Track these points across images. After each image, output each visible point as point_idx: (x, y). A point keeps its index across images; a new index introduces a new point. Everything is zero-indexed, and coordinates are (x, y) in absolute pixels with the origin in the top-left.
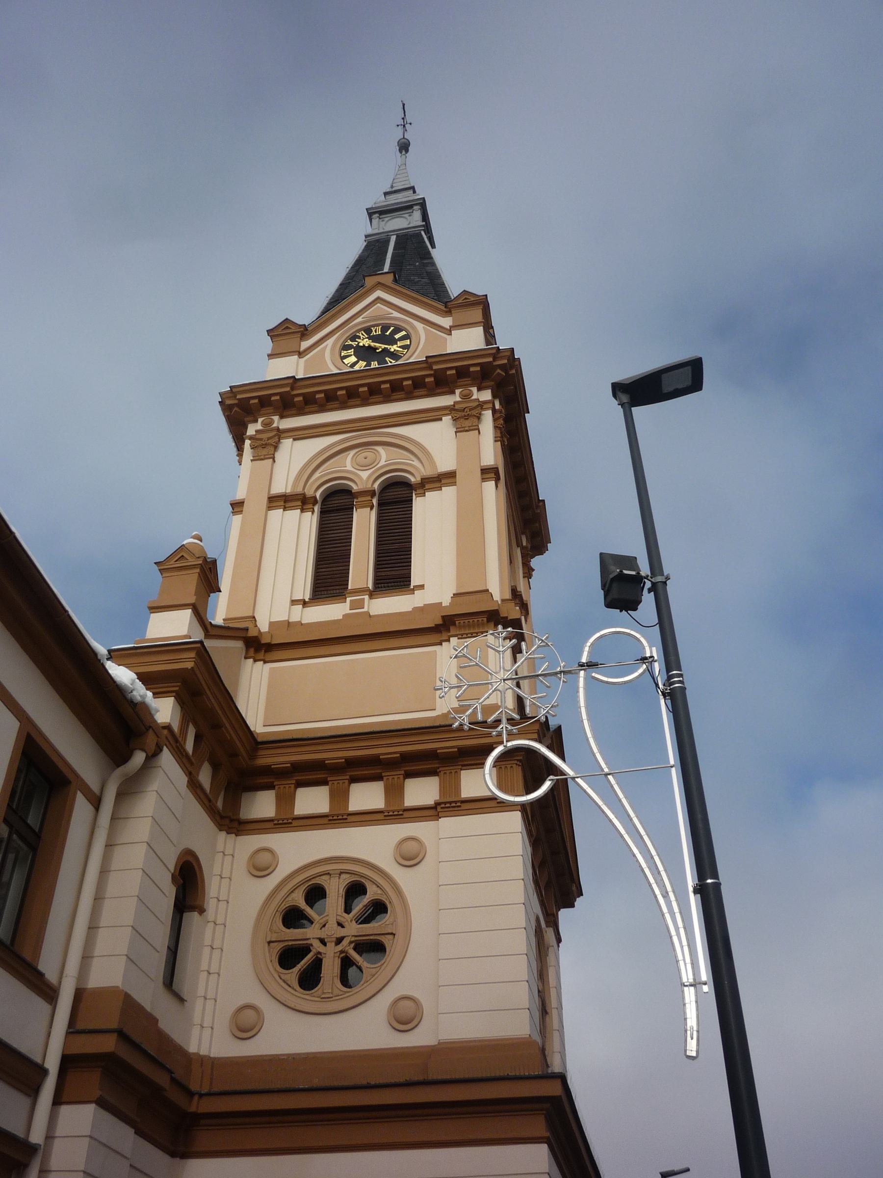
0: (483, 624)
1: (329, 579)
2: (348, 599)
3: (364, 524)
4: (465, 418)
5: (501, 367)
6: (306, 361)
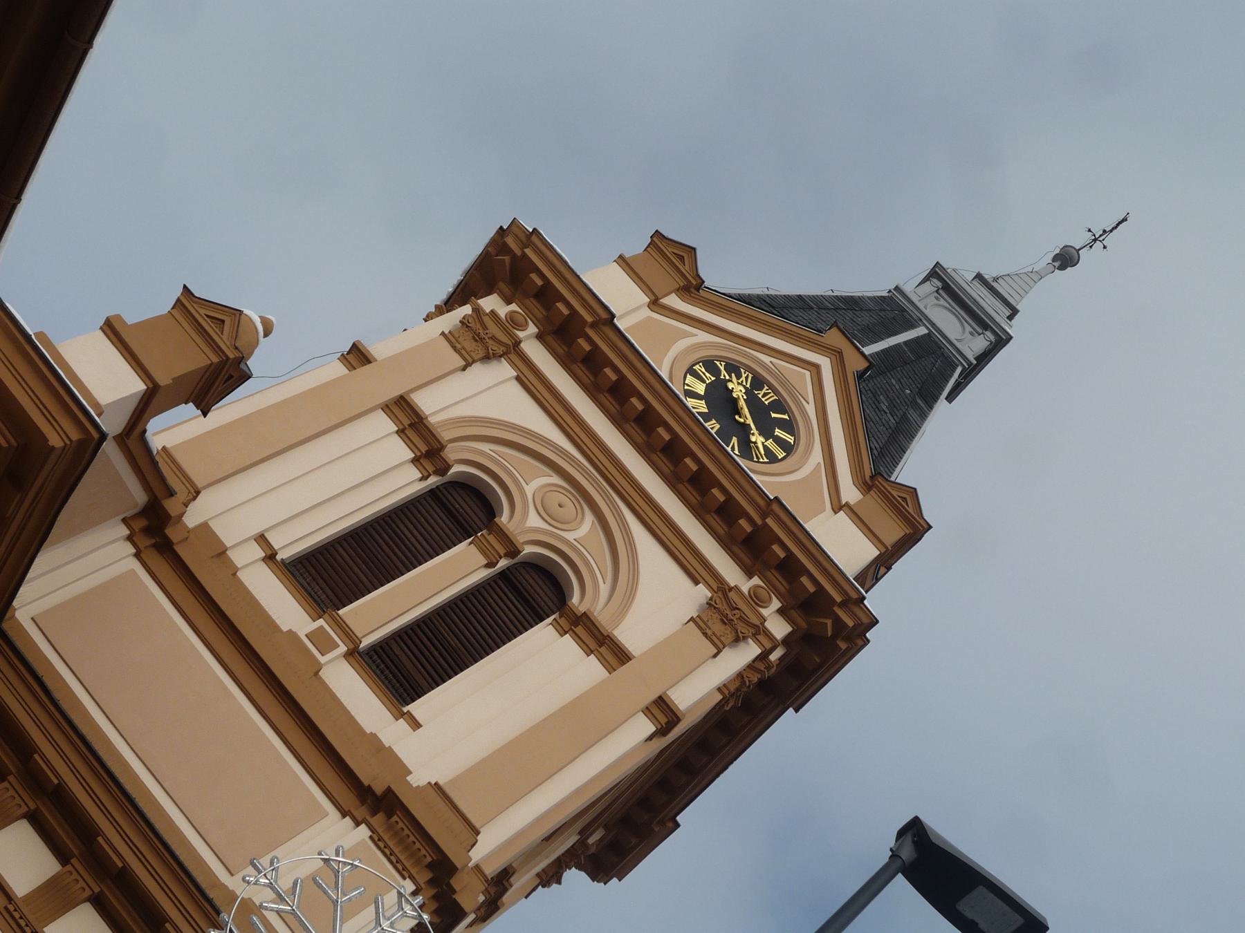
0: (418, 862)
2: (321, 622)
3: (457, 570)
4: (723, 619)
5: (838, 622)
6: (649, 318)
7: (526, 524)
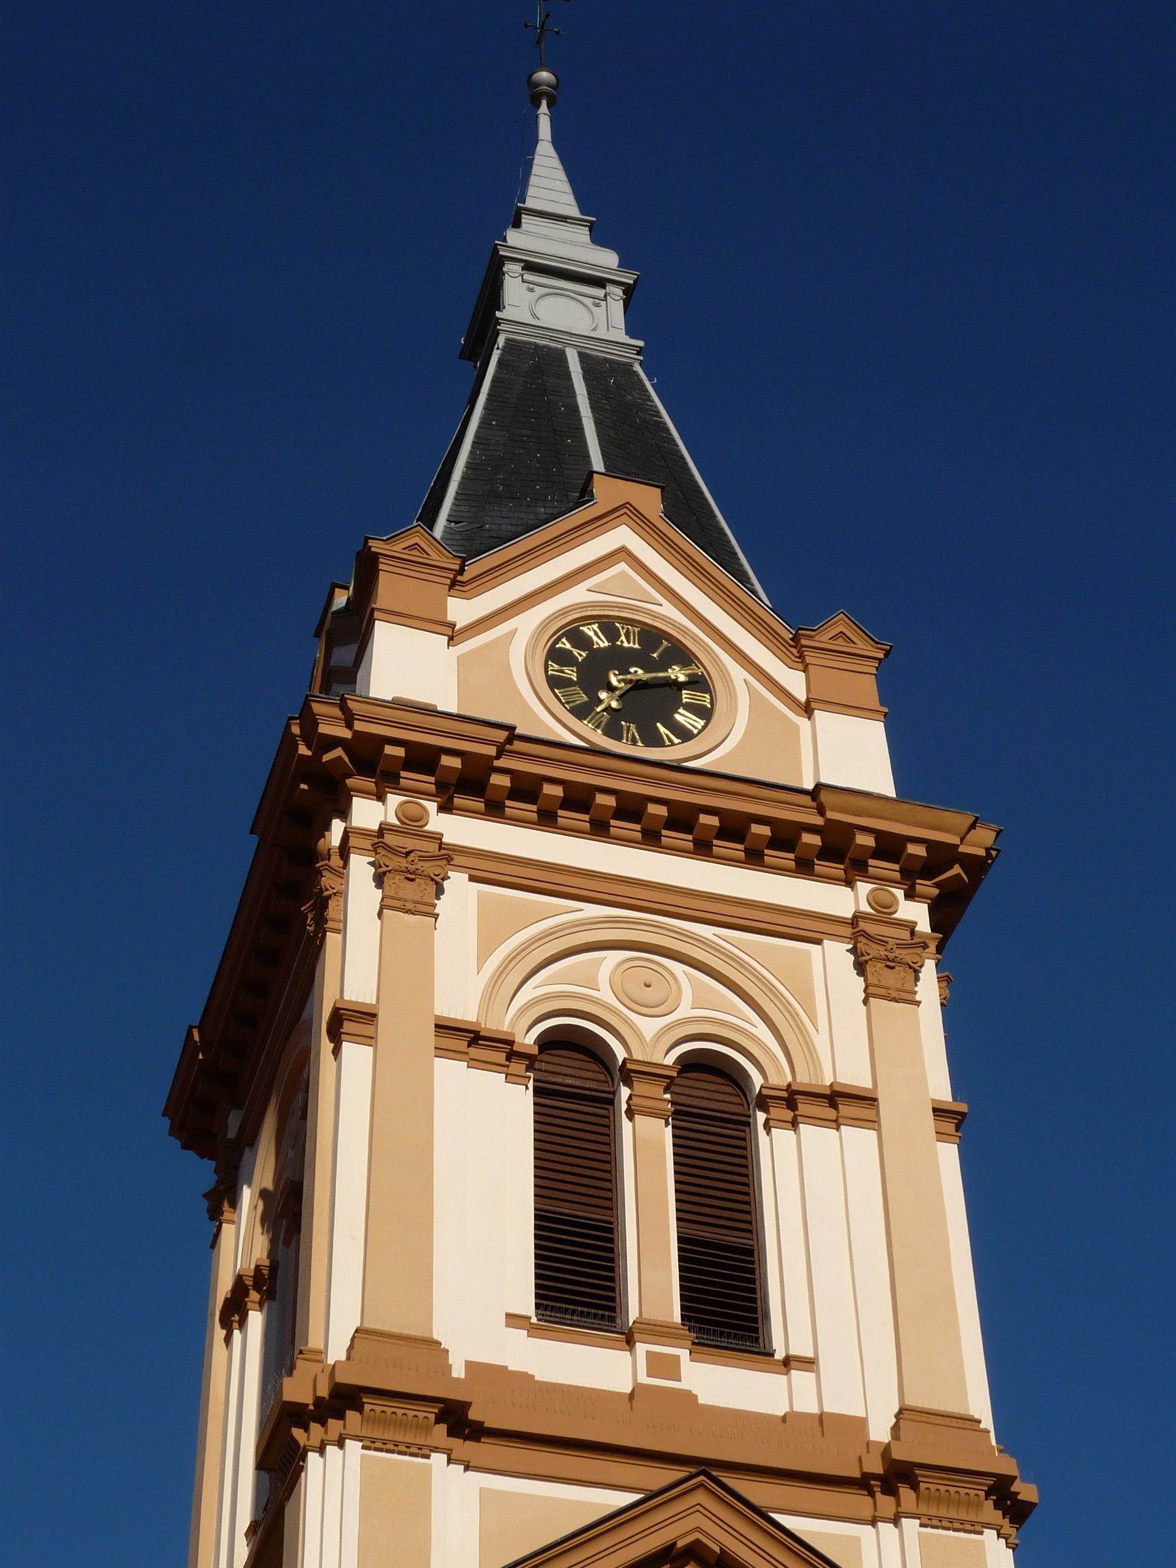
1: (575, 1278)
4: (878, 957)
7: (648, 1037)
